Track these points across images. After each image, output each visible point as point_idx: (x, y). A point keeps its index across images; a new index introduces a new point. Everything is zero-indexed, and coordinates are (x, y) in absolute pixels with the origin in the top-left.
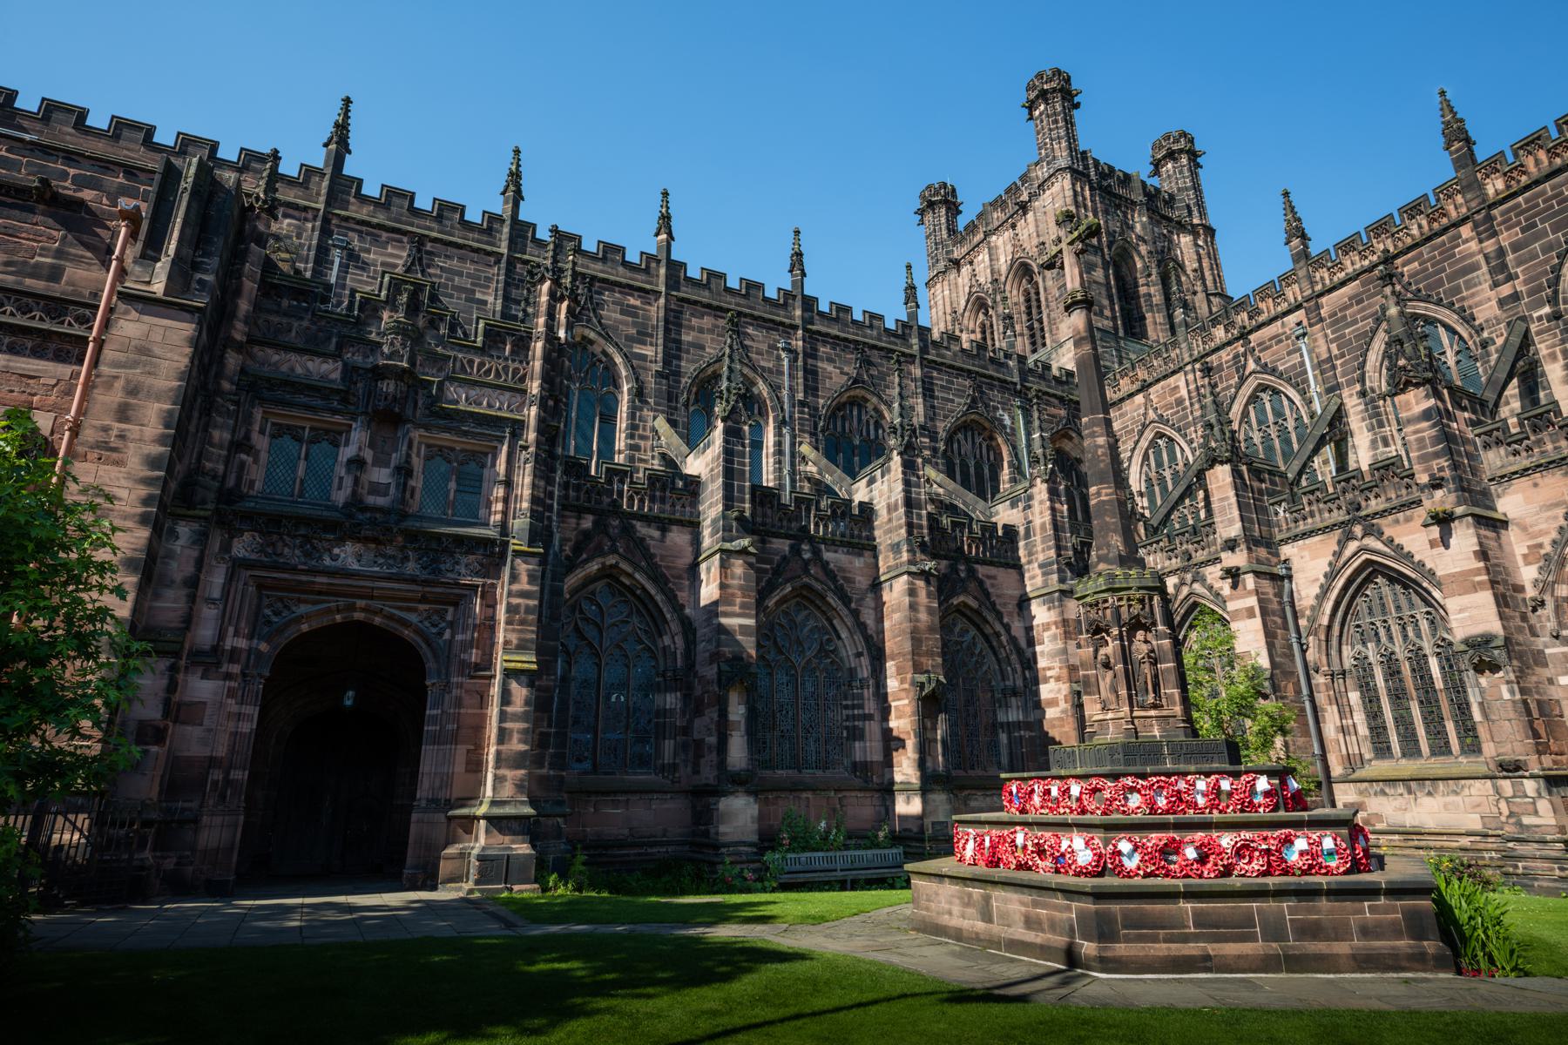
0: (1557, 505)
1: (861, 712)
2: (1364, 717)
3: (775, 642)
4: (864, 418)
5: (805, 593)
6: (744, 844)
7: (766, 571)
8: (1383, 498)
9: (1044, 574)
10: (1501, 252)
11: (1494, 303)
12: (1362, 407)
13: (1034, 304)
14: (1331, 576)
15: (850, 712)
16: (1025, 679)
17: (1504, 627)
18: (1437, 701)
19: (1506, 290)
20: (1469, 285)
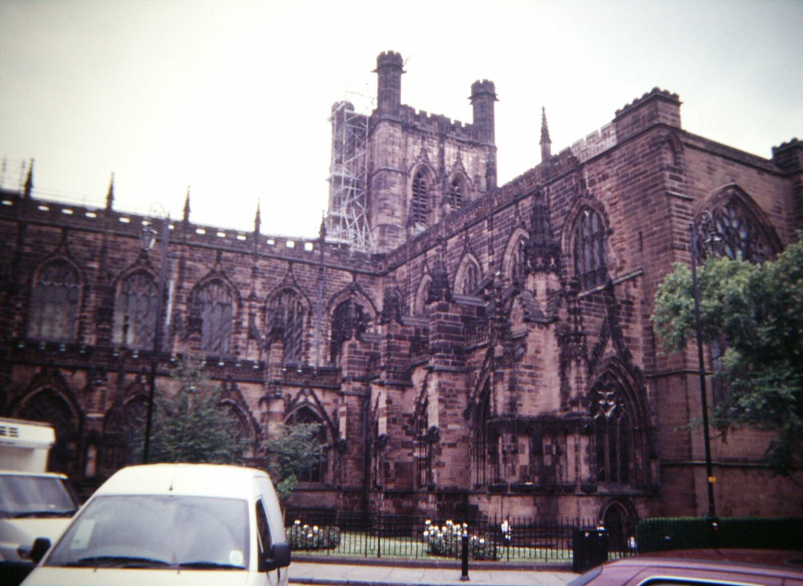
17: (388, 432)
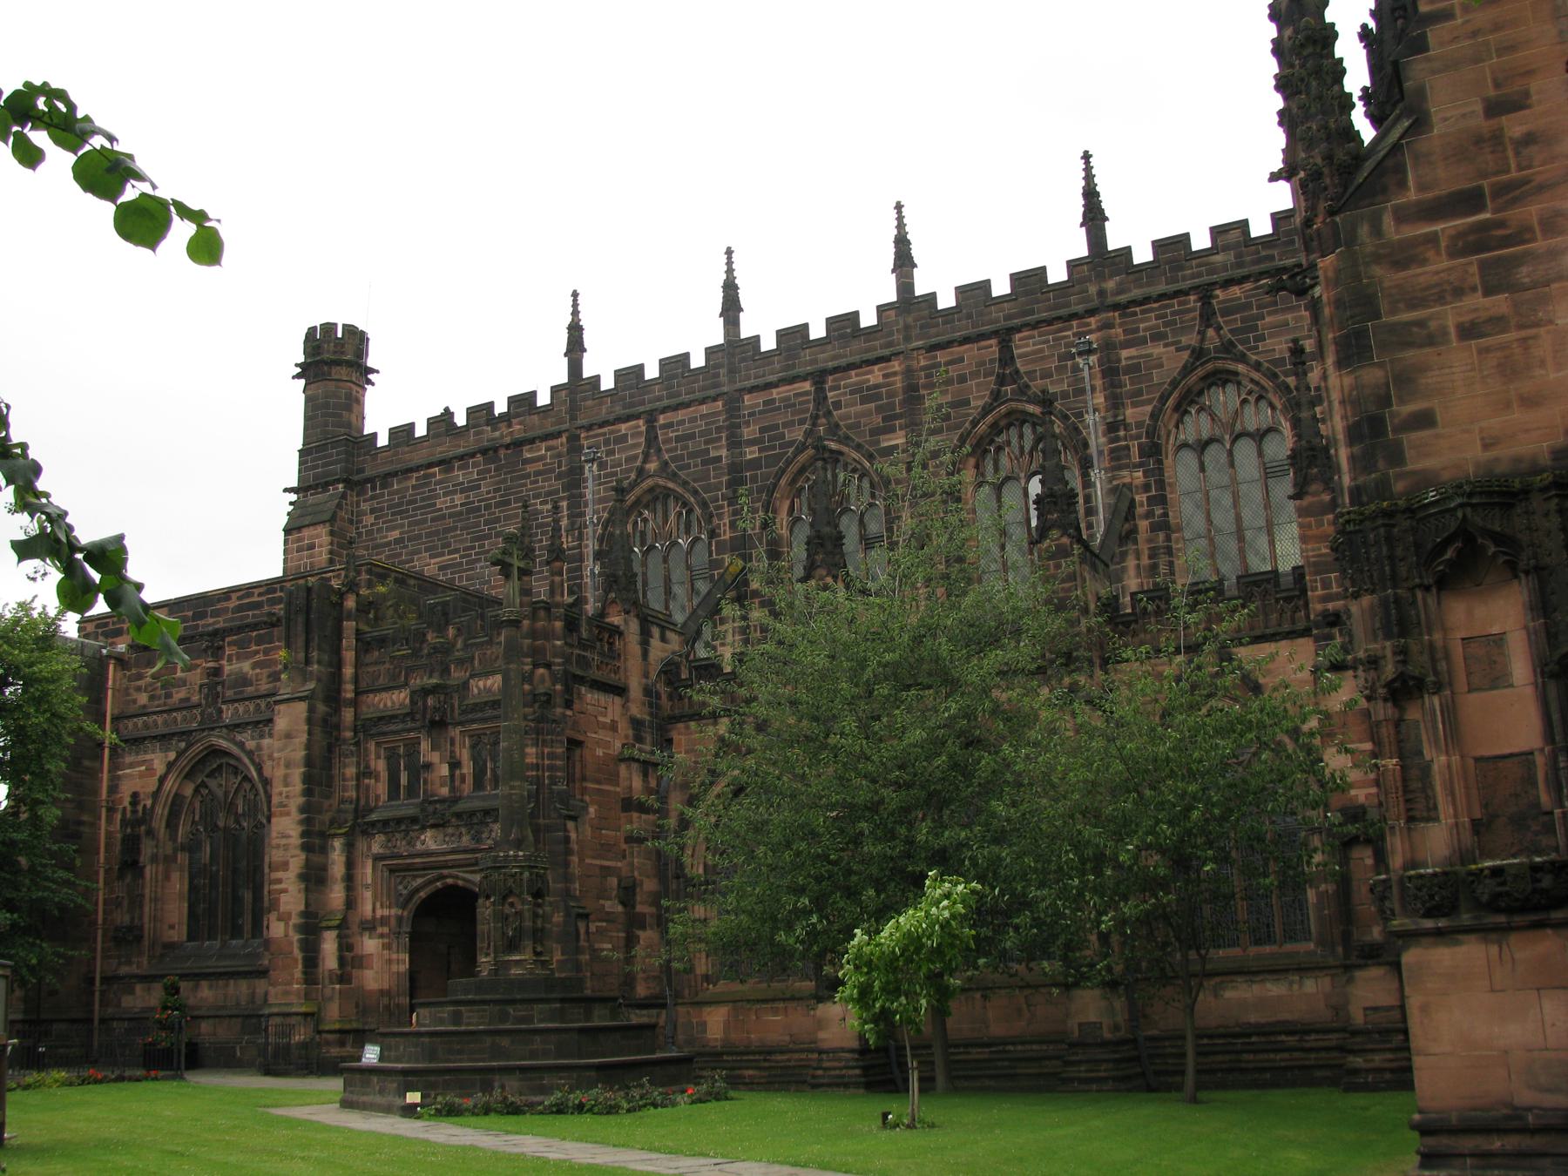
6: (843, 1050)
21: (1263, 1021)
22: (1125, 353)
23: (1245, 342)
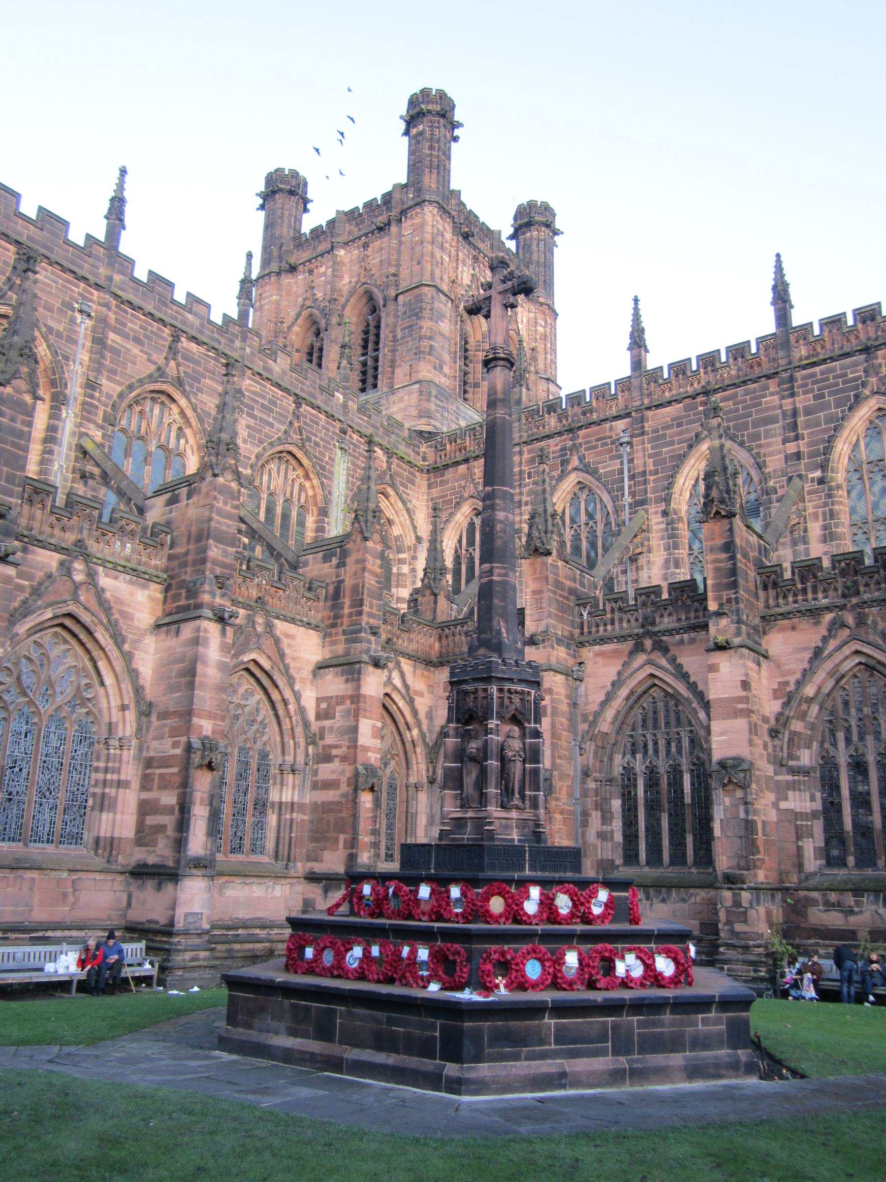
0: (804, 649)
1: (115, 777)
2: (620, 824)
3: (19, 679)
4: (166, 421)
5: (68, 622)
7: (21, 588)
8: (675, 618)
9: (347, 641)
10: (795, 413)
11: (782, 456)
12: (663, 526)
13: (372, 338)
14: (616, 685)
15: (100, 776)
16: (307, 755)
17: (751, 753)
18: (684, 815)
19: (791, 448)
20: (768, 435)
21: (247, 917)
22: (112, 336)
23: (191, 386)
